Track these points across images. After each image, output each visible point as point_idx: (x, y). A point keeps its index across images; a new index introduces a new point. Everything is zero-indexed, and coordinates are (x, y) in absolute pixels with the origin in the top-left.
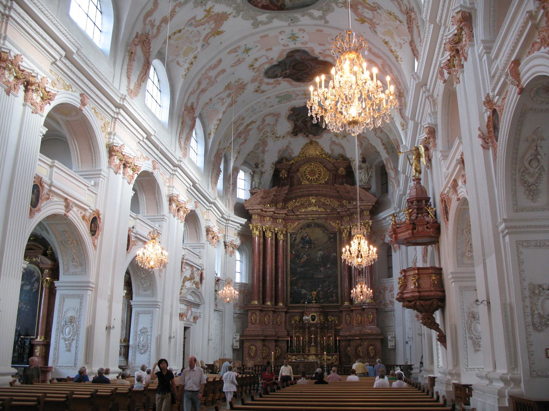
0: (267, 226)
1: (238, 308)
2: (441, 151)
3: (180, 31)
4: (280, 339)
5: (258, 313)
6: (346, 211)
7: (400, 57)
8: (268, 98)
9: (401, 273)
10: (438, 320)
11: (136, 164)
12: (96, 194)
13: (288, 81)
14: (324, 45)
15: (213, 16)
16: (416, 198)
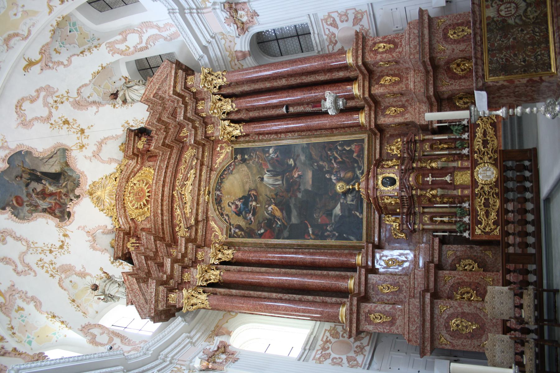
0: (198, 276)
1: (360, 359)
4: (436, 259)
5: (366, 307)
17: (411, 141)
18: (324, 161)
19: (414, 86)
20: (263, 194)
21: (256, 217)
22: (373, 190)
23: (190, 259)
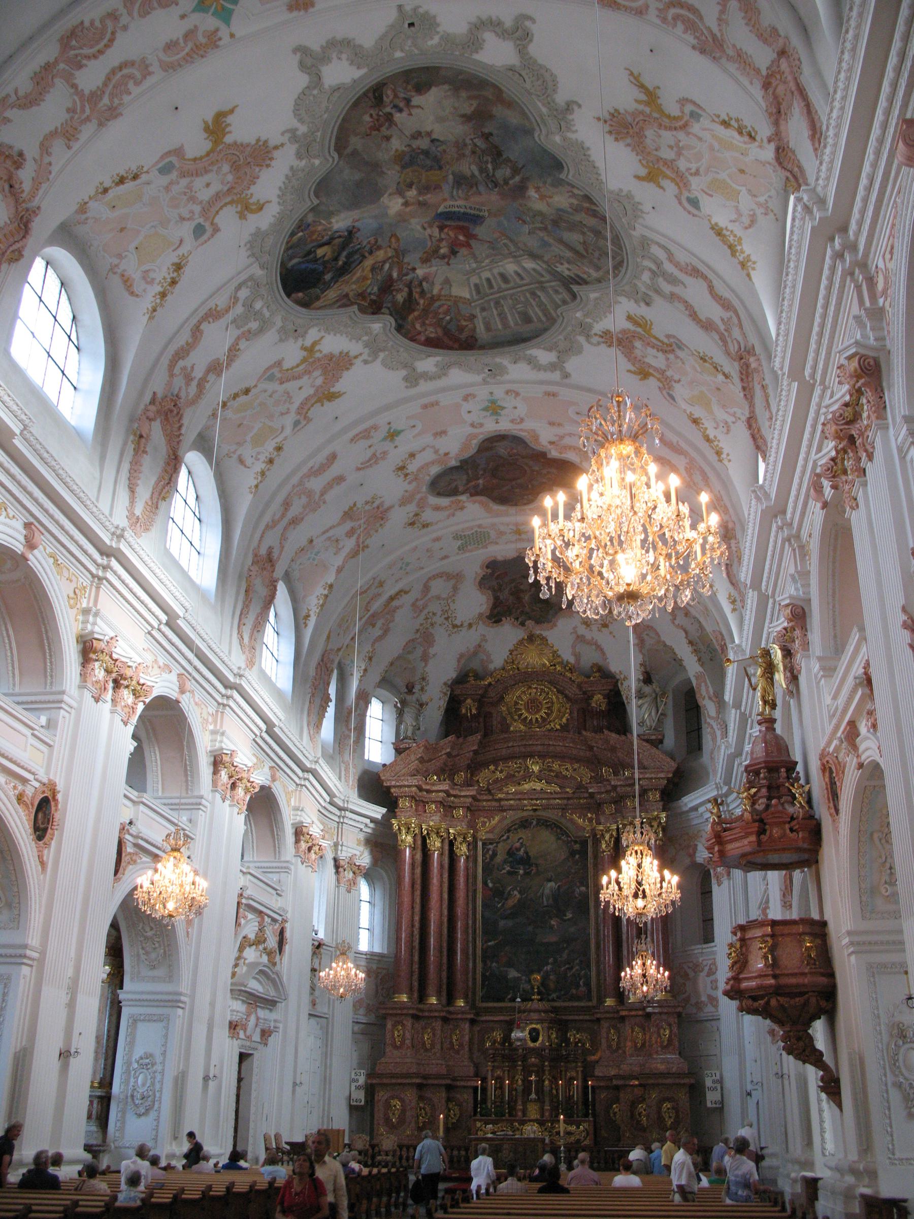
1: (362, 1011)
2: (820, 659)
3: (247, 391)
4: (458, 1083)
5: (409, 1023)
6: (607, 792)
7: (725, 451)
8: (437, 539)
9: (734, 933)
10: (821, 1044)
11: (142, 681)
12: (50, 746)
13: (481, 503)
14: (559, 425)
15: (319, 360)
16: (765, 762)
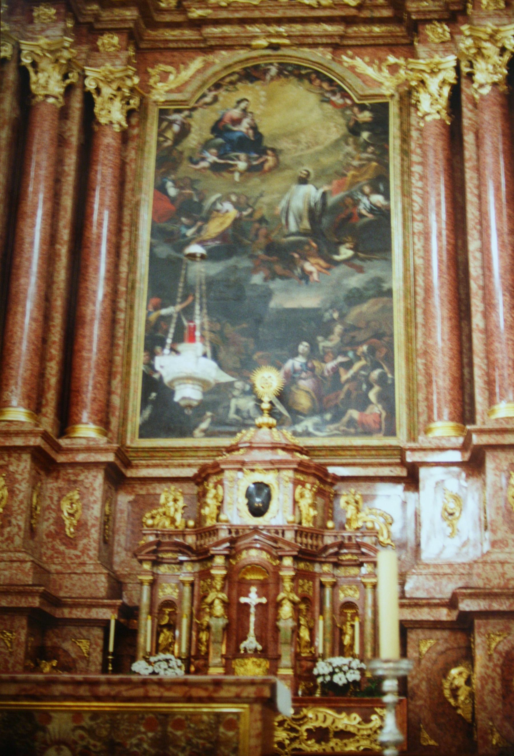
17: (363, 554)
18: (342, 335)
19: (493, 562)
20: (264, 187)
21: (209, 172)
22: (238, 462)
23: (97, 17)
